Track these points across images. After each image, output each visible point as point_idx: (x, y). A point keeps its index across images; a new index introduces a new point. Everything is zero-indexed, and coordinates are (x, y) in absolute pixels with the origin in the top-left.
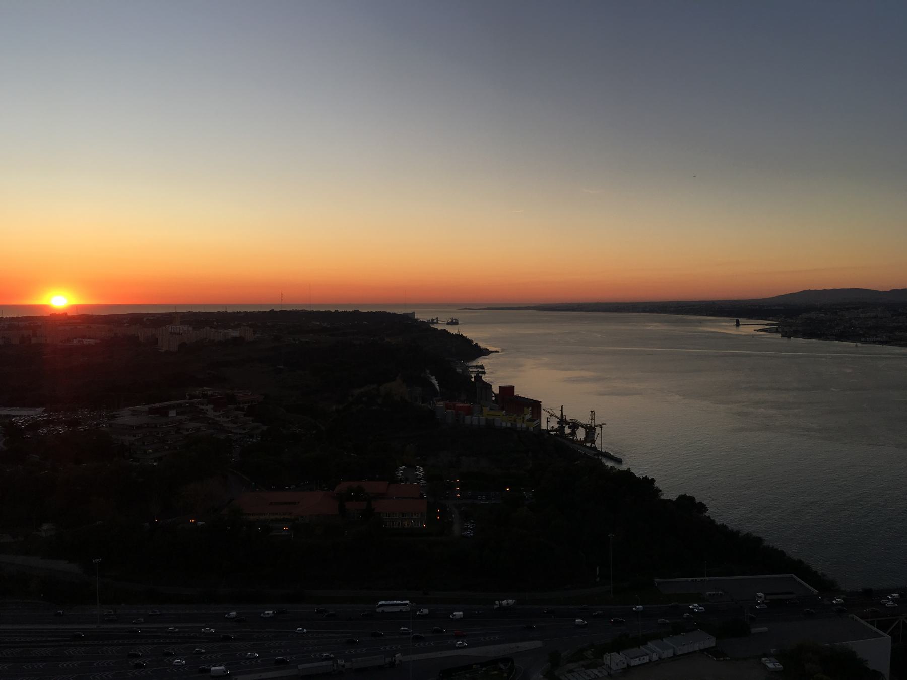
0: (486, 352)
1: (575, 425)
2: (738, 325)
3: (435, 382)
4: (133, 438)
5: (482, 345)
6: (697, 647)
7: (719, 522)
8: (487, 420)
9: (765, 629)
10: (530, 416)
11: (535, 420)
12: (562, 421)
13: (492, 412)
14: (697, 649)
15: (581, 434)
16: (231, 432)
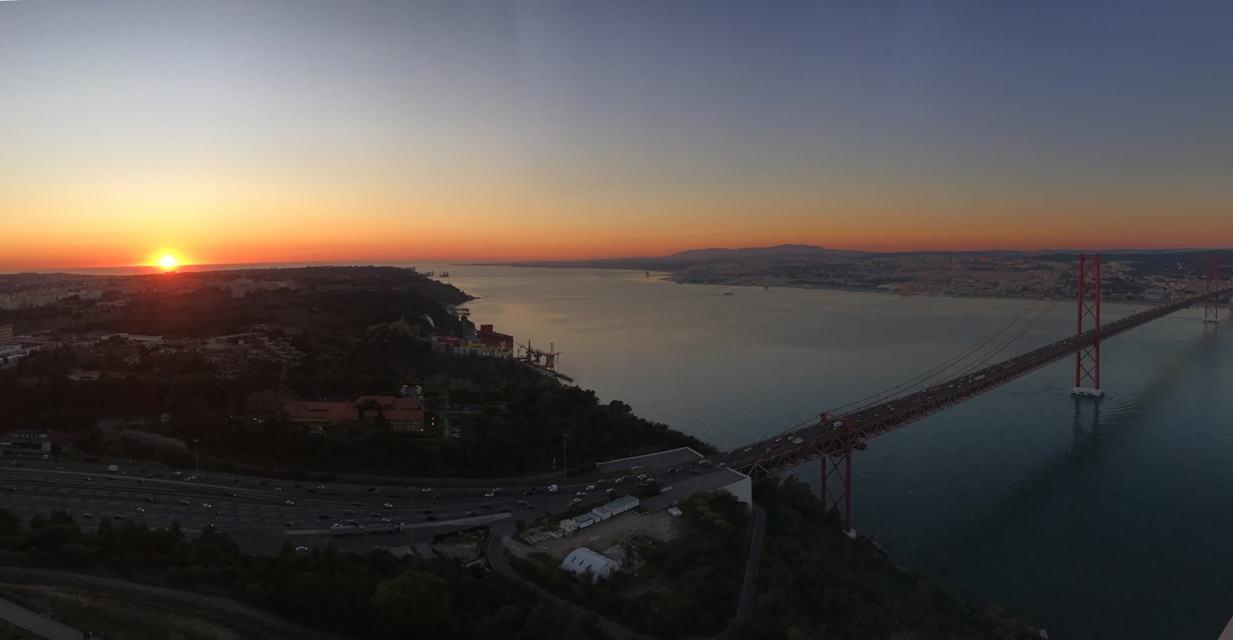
0: (470, 298)
1: (539, 355)
2: (648, 276)
3: (431, 322)
4: (218, 359)
5: (467, 293)
6: (626, 508)
7: (639, 418)
8: (471, 351)
9: (670, 488)
10: (504, 348)
11: (508, 351)
12: (529, 351)
13: (475, 345)
14: (626, 509)
15: (543, 360)
16: (280, 357)
